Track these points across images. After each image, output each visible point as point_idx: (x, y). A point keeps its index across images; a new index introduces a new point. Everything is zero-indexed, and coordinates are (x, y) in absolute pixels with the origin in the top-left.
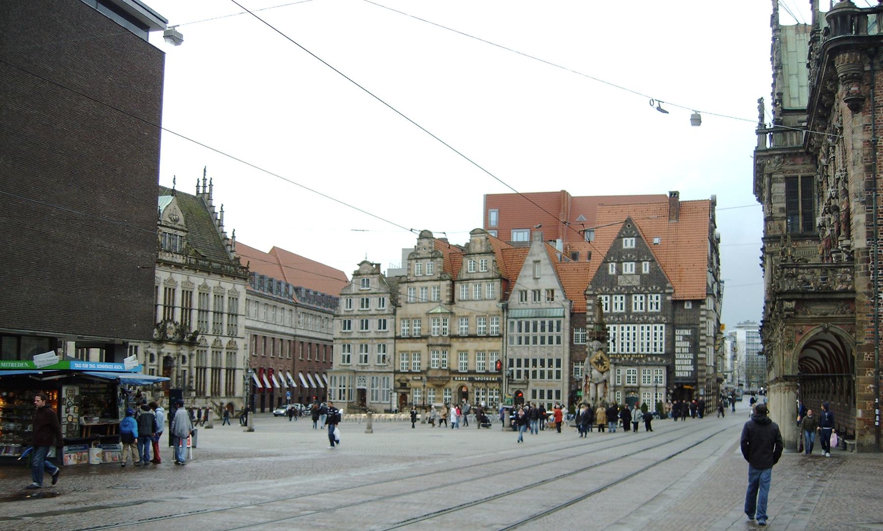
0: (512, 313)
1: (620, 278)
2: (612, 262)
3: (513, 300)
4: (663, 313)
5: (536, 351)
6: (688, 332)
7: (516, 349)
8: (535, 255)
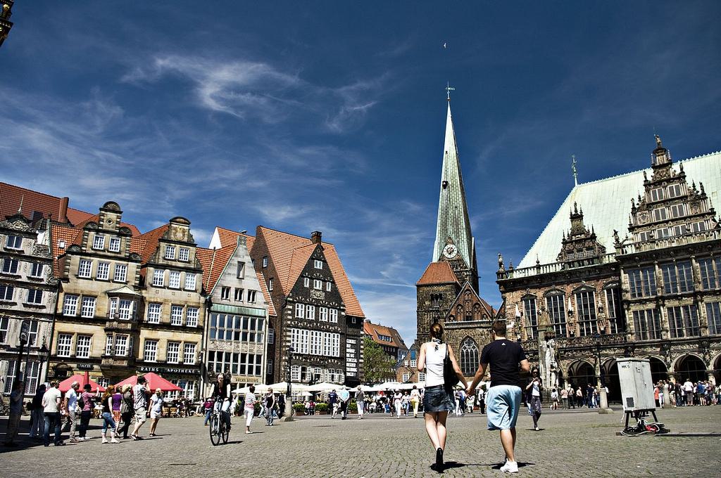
0: (215, 307)
1: (312, 291)
2: (307, 277)
4: (339, 324)
5: (238, 347)
6: (353, 342)
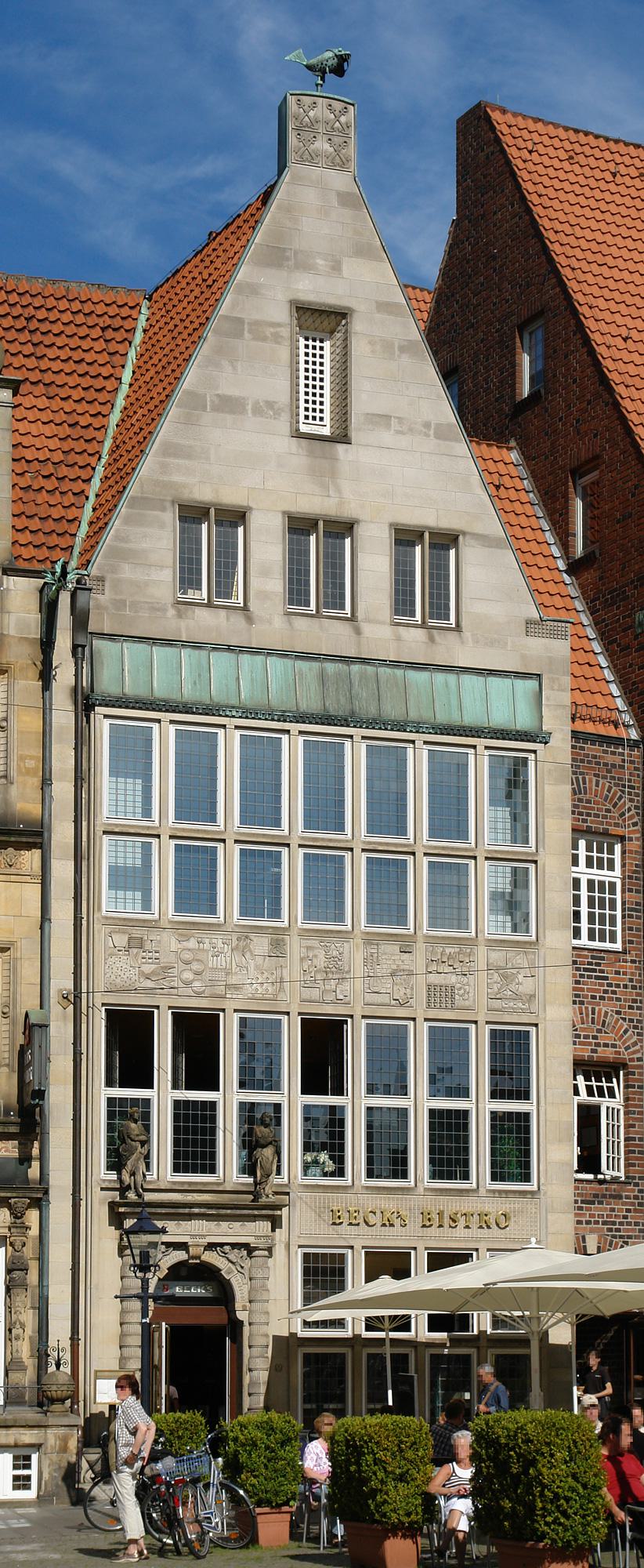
3: (127, 572)
5: (336, 970)
7: (170, 942)
8: (303, 264)
